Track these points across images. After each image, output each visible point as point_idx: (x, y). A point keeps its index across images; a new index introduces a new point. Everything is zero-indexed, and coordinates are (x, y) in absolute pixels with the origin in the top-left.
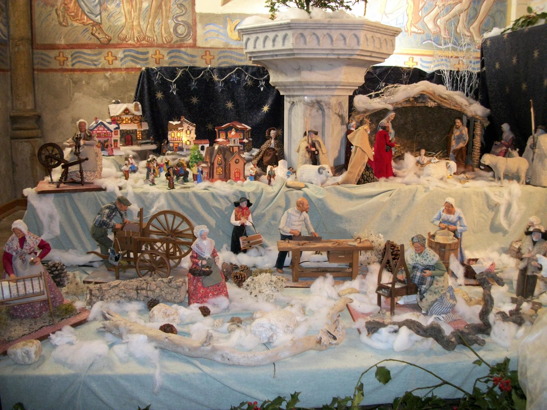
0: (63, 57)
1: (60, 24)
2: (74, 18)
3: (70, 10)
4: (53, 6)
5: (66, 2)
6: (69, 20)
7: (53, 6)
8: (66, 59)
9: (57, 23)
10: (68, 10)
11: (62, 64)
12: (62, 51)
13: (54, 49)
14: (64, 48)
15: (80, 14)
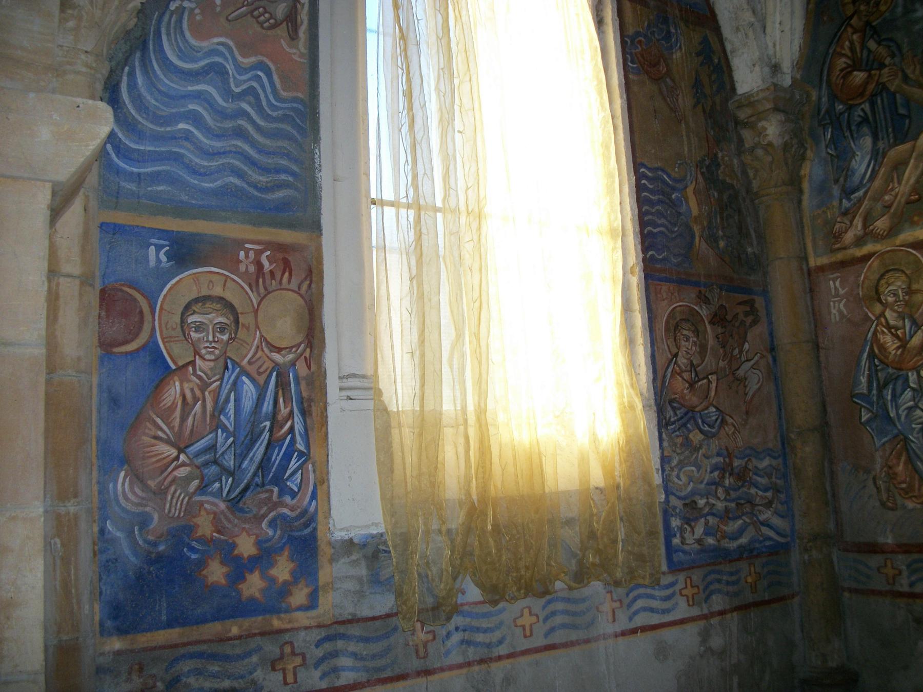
0: (893, 568)
1: (883, 504)
2: (907, 493)
3: (899, 479)
4: (867, 471)
5: (890, 464)
6: (898, 497)
7: (867, 471)
8: (897, 572)
9: (877, 504)
10: (895, 479)
11: (891, 581)
12: (889, 555)
13: (875, 552)
14: (893, 552)
15: (917, 486)
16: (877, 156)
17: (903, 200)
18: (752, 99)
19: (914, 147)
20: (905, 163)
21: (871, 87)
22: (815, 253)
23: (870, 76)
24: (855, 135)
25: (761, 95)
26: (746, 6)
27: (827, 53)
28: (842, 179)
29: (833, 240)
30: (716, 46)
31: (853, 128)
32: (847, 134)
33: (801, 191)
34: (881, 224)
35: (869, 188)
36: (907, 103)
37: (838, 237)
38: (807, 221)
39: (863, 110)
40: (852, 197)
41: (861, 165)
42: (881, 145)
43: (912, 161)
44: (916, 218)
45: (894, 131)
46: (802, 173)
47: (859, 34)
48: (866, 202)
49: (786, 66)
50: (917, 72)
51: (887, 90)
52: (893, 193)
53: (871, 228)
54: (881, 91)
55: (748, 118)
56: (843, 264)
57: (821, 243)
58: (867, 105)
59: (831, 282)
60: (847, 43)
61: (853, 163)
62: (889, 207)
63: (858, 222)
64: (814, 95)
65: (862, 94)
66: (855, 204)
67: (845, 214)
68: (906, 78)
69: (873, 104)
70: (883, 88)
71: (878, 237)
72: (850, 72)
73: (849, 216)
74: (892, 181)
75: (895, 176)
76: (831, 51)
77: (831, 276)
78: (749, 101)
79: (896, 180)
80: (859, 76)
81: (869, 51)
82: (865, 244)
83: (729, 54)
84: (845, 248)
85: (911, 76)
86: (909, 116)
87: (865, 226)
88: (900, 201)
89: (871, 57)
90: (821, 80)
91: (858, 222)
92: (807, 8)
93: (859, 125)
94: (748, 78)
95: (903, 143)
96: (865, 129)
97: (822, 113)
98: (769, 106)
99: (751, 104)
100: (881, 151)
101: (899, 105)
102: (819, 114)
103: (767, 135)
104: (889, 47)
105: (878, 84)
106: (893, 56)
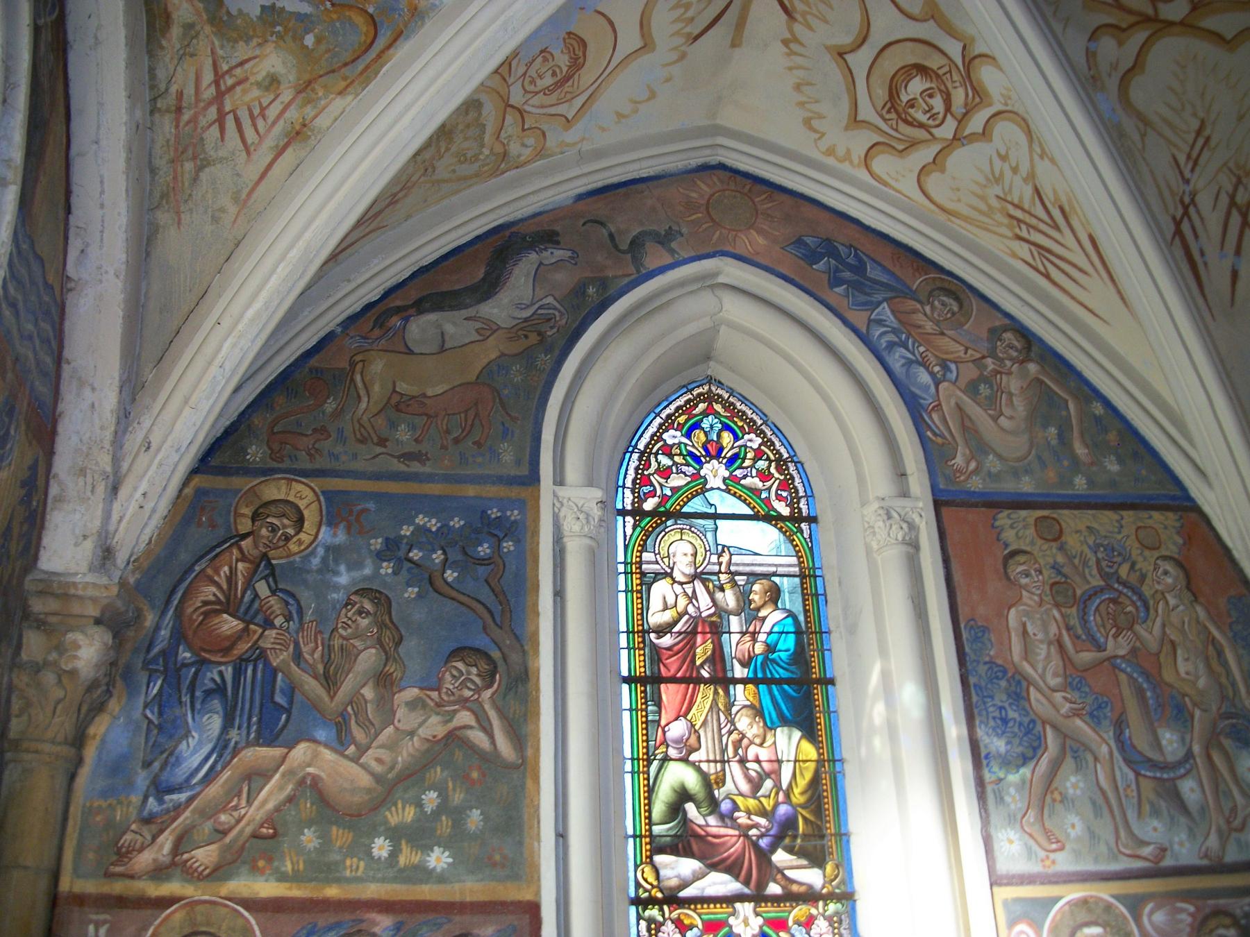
16: (222, 747)
17: (249, 830)
18: (72, 591)
19: (284, 758)
20: (266, 776)
21: (243, 647)
22: (75, 870)
23: (246, 629)
24: (198, 706)
25: (90, 592)
26: (107, 445)
27: (190, 569)
28: (157, 765)
29: (115, 858)
30: (41, 482)
31: (198, 693)
32: (186, 699)
33: (80, 761)
34: (205, 856)
35: (199, 794)
36: (291, 691)
37: (123, 855)
38: (75, 811)
39: (221, 673)
40: (167, 798)
41: (194, 752)
42: (234, 735)
43: (277, 776)
44: (261, 863)
45: (260, 721)
46: (91, 730)
47: (247, 565)
48: (187, 813)
49: (121, 557)
50: (317, 655)
51: (267, 663)
52: (236, 814)
53: (186, 856)
54: (256, 660)
55: (46, 614)
56: (121, 902)
57: (91, 856)
58: (230, 669)
59: (91, 928)
60: (226, 569)
61: (183, 746)
62: (224, 833)
63: (166, 841)
64: (150, 619)
65: (226, 651)
66: (168, 811)
67: (148, 820)
68: (298, 657)
69: (238, 673)
70: (261, 655)
71: (191, 874)
72: (218, 612)
73: (154, 828)
74: (239, 795)
75: (245, 790)
76: (197, 568)
77: (94, 917)
78: (57, 588)
79: (244, 795)
80: (229, 624)
81: (256, 595)
82: (168, 878)
83: (50, 501)
84: (132, 877)
85: (307, 657)
86: (289, 712)
87: (176, 850)
88: (242, 831)
89: (256, 605)
90: (168, 602)
91: (166, 841)
92: (181, 491)
93: (208, 693)
94: (66, 550)
95: (270, 743)
96: (216, 703)
97: (156, 650)
98: (93, 611)
99: (66, 597)
100: (232, 743)
101: (278, 687)
102: (148, 650)
103: (75, 657)
104: (287, 603)
105: (255, 646)
106: (289, 618)
